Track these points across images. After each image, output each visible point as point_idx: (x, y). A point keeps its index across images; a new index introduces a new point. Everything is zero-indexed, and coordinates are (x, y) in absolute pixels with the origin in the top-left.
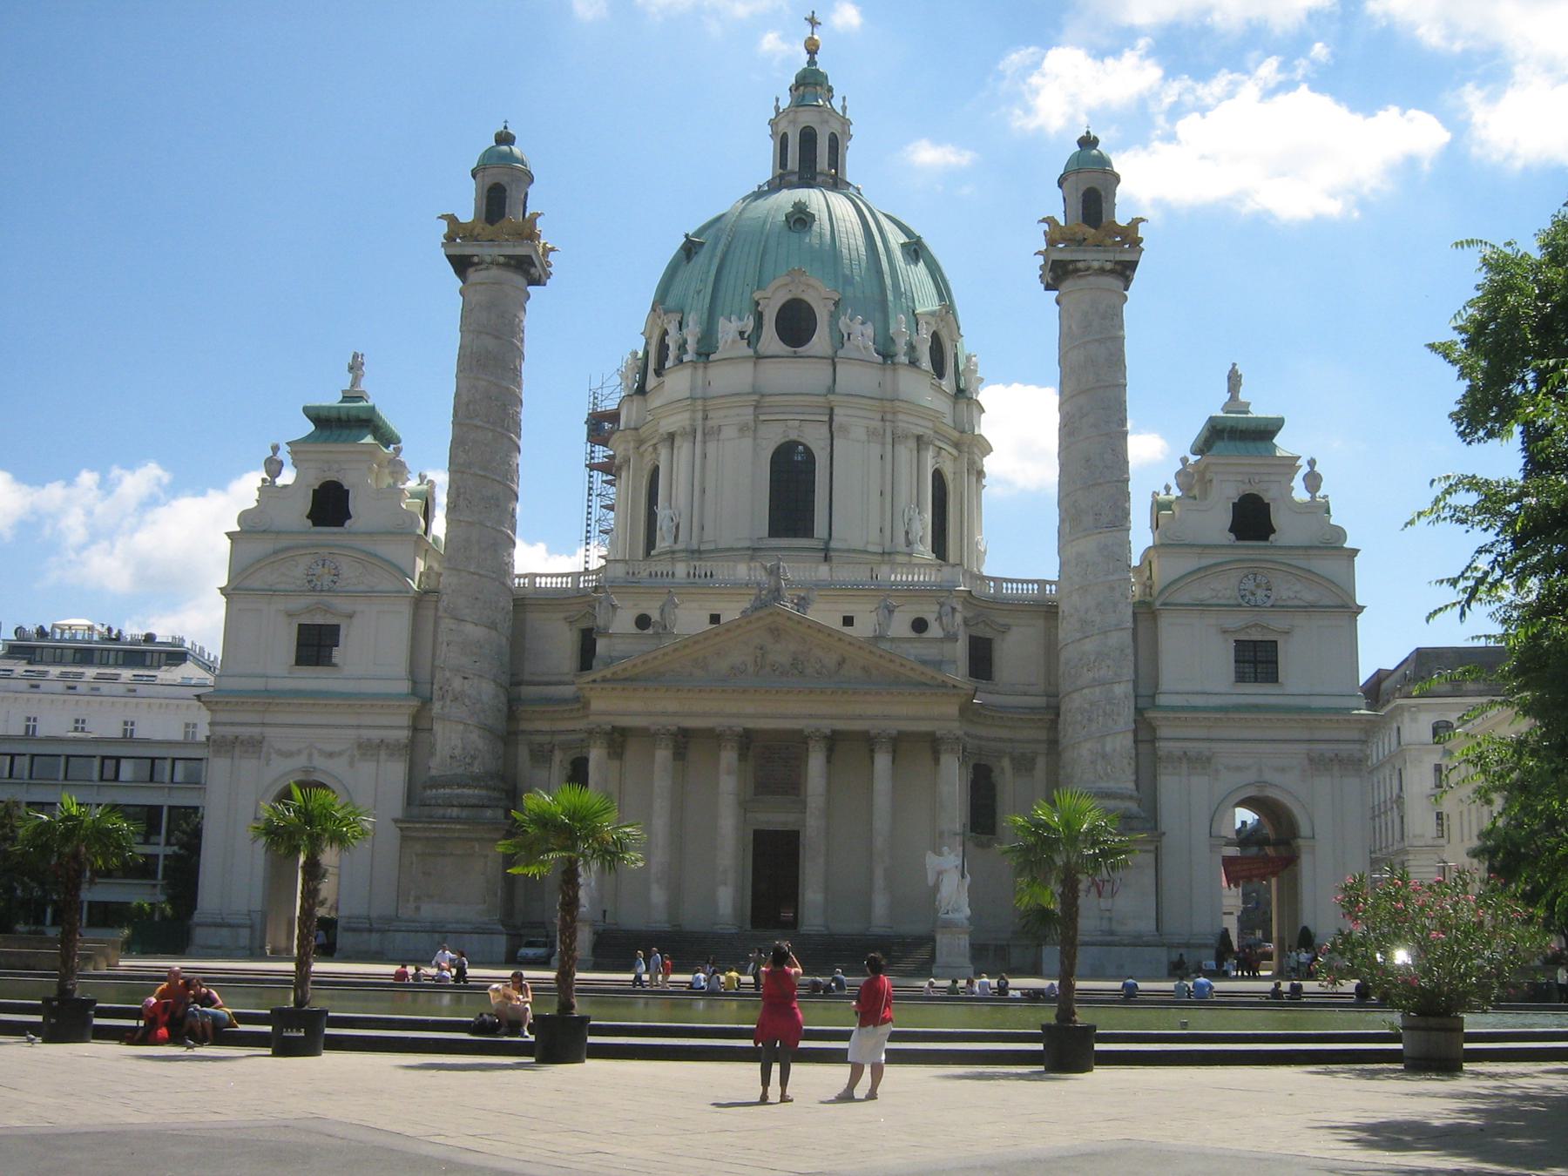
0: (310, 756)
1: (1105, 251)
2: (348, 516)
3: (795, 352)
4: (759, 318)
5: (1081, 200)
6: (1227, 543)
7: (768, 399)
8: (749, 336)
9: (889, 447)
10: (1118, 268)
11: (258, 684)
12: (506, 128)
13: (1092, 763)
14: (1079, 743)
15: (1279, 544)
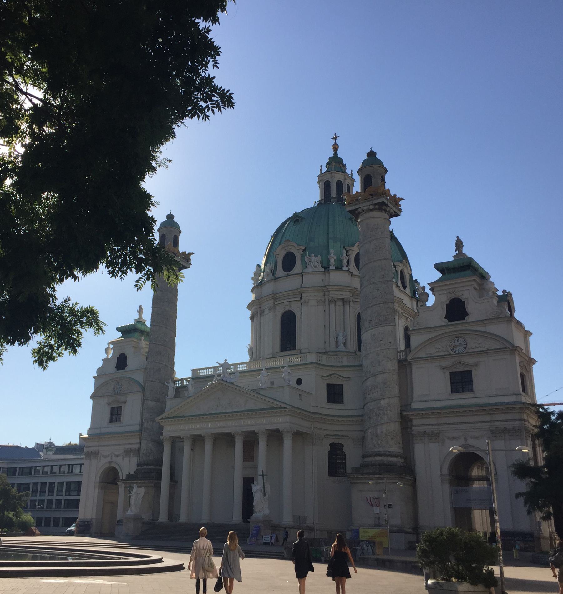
0: (112, 457)
1: (368, 201)
2: (127, 365)
3: (288, 274)
4: (276, 262)
5: (363, 181)
6: (443, 324)
7: (278, 295)
8: (273, 271)
9: (327, 307)
10: (377, 207)
11: (98, 431)
12: (170, 213)
13: (372, 439)
14: (367, 430)
15: (467, 321)
